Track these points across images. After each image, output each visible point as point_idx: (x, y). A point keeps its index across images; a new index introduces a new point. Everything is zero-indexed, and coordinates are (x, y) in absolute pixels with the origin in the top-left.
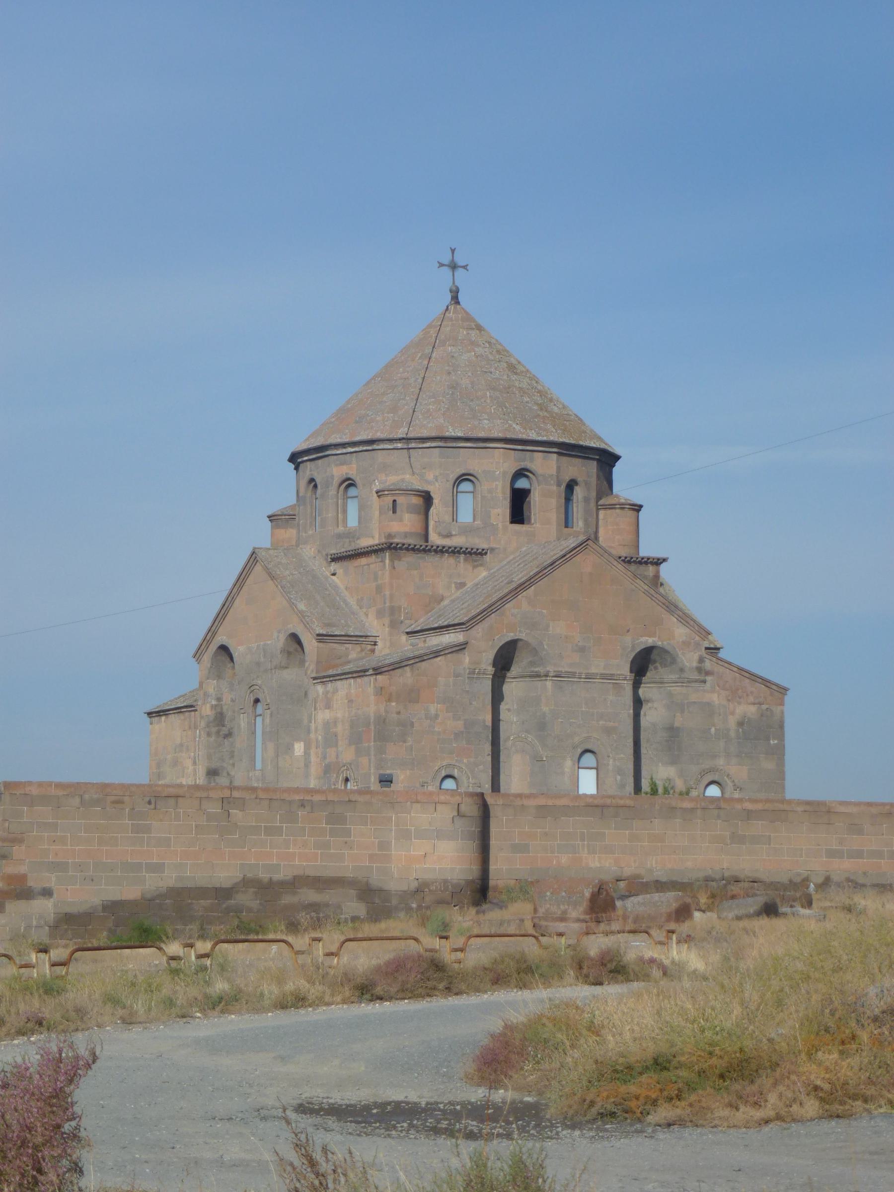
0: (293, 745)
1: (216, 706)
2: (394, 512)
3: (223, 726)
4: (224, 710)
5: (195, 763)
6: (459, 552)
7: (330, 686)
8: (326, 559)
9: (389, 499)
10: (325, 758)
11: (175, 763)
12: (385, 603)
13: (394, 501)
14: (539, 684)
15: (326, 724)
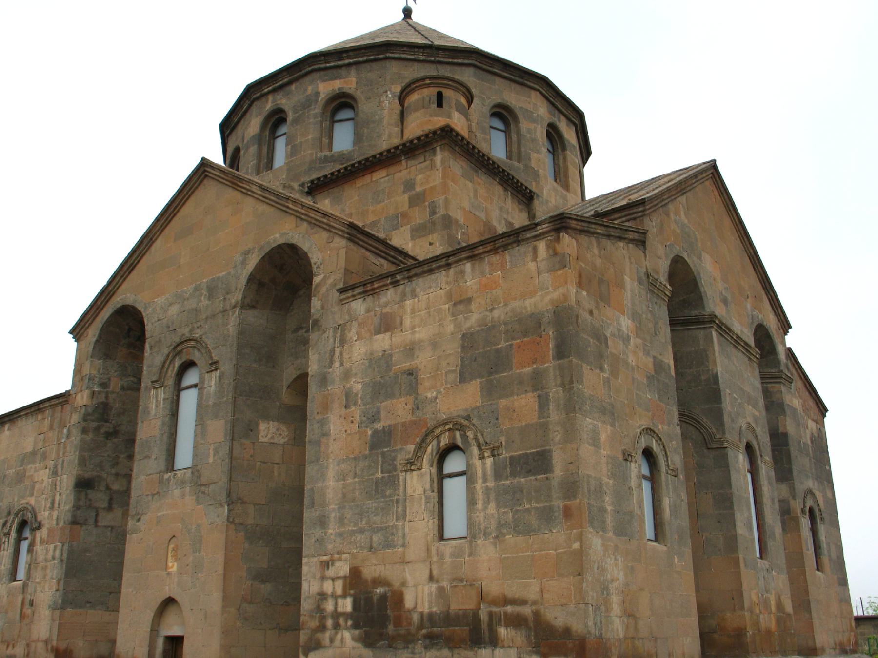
0: (258, 425)
1: (99, 393)
2: (440, 104)
3: (107, 421)
4: (111, 401)
5: (55, 473)
6: (506, 182)
7: (390, 294)
8: (302, 192)
9: (433, 91)
10: (374, 418)
11: (20, 478)
12: (433, 213)
13: (440, 95)
14: (701, 334)
15: (380, 363)
